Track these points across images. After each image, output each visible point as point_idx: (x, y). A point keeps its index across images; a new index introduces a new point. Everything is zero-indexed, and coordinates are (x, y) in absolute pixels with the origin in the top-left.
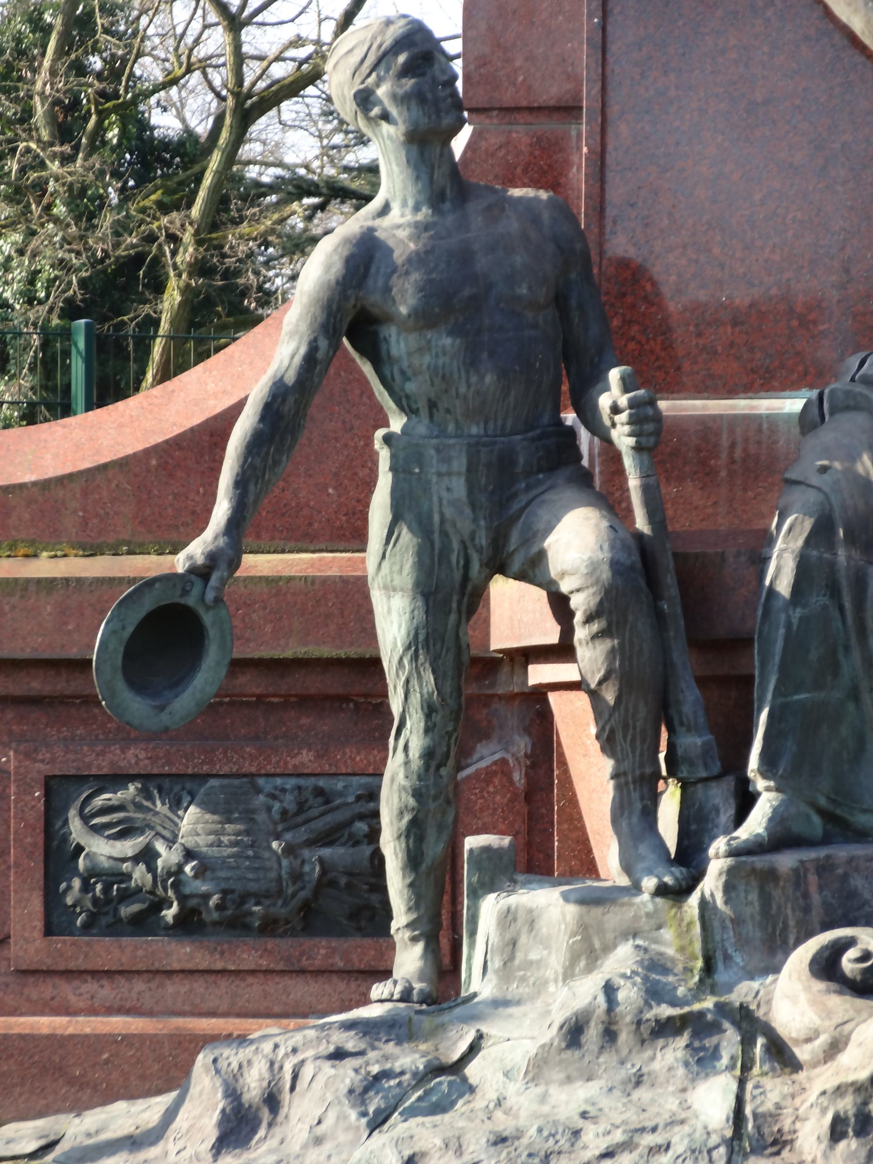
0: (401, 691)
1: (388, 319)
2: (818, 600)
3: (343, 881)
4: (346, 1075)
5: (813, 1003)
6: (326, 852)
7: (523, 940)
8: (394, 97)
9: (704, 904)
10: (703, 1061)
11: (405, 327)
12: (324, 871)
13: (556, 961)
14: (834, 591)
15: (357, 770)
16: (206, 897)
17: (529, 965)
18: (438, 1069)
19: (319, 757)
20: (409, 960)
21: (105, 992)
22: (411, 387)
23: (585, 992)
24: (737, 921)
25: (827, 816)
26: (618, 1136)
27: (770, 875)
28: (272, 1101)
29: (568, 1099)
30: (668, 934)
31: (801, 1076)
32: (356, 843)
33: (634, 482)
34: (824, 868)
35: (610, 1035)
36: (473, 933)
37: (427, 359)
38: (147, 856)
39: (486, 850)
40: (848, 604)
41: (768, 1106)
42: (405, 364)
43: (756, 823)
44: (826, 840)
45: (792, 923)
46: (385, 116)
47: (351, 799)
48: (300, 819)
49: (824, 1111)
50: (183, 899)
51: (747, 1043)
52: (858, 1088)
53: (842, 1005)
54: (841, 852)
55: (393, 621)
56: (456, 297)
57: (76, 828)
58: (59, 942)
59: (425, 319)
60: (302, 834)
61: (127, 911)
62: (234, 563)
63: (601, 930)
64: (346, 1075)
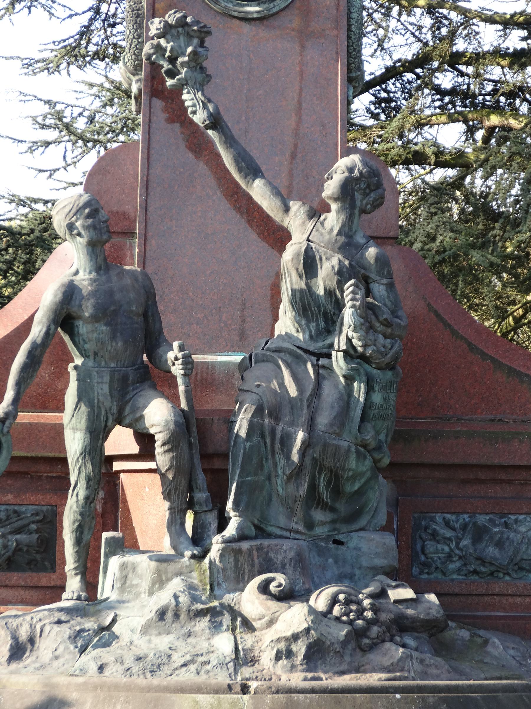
0: (76, 472)
1: (79, 318)
2: (256, 439)
3: (25, 549)
4: (66, 631)
5: (262, 604)
6: (18, 537)
7: (130, 575)
8: (83, 226)
9: (211, 562)
10: (216, 627)
11: (86, 321)
12: (18, 545)
13: (145, 584)
14: (263, 436)
15: (31, 503)
17: (132, 586)
18: (103, 629)
19: (15, 497)
20: (74, 584)
22: (87, 346)
23: (164, 597)
24: (224, 570)
25: (257, 527)
26: (188, 658)
27: (239, 552)
28: (32, 641)
29: (163, 642)
30: (195, 574)
31: (257, 633)
32: (31, 533)
33: (181, 389)
34: (260, 548)
35: (177, 616)
36: (105, 572)
37: (95, 335)
39: (113, 538)
40: (268, 441)
41: (248, 646)
42: (85, 337)
43: (231, 530)
44: (256, 538)
45: (247, 571)
46: (79, 235)
47: (29, 515)
48: (7, 523)
49: (273, 648)
51: (234, 620)
52: (287, 639)
53: (274, 605)
54: (266, 542)
55: (74, 443)
56: (108, 311)
59: (95, 319)
60: (8, 529)
62: (15, 417)
63: (166, 572)
64: (66, 631)
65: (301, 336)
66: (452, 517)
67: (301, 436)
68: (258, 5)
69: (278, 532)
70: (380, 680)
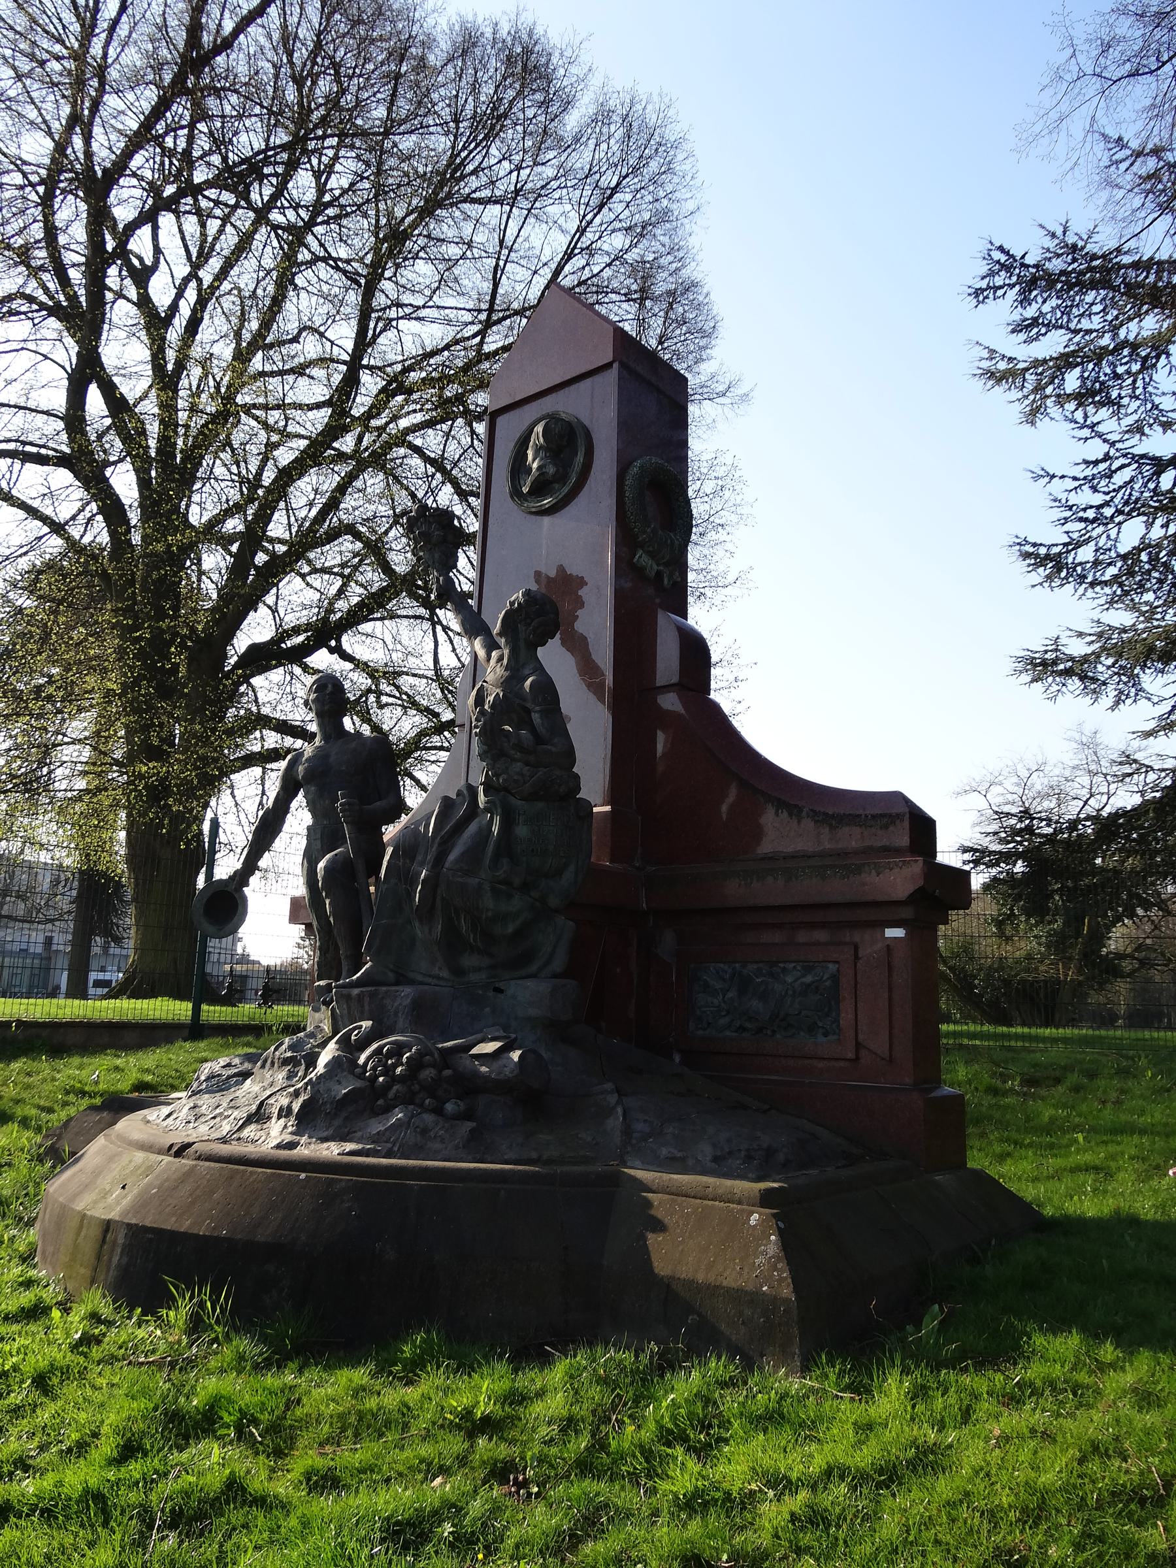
35: (273, 1064)
66: (726, 967)
69: (420, 978)
70: (352, 1153)
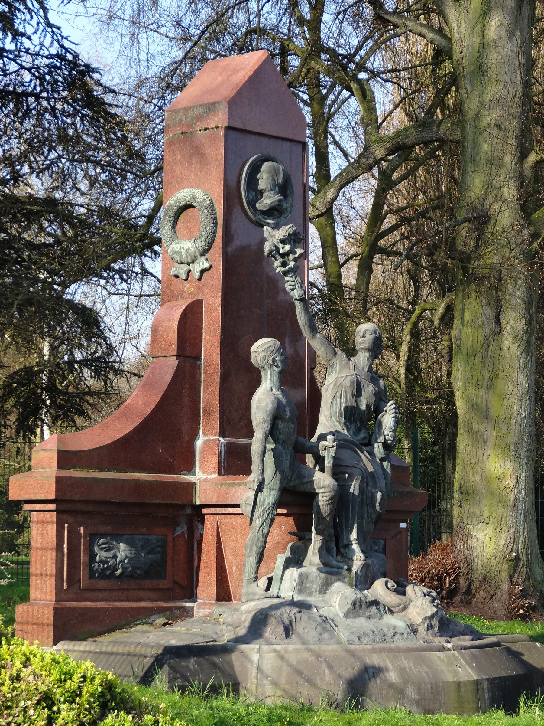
7: (305, 581)
16: (128, 568)
21: (100, 595)
28: (291, 624)
35: (361, 606)
38: (115, 557)
42: (281, 431)
46: (277, 366)
50: (123, 569)
57: (96, 549)
58: (93, 581)
61: (108, 573)
65: (345, 432)
67: (379, 495)
68: (272, 219)
